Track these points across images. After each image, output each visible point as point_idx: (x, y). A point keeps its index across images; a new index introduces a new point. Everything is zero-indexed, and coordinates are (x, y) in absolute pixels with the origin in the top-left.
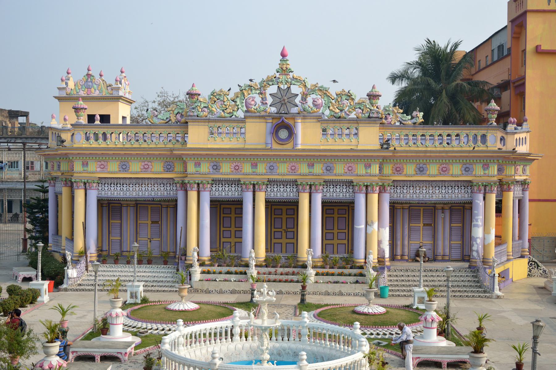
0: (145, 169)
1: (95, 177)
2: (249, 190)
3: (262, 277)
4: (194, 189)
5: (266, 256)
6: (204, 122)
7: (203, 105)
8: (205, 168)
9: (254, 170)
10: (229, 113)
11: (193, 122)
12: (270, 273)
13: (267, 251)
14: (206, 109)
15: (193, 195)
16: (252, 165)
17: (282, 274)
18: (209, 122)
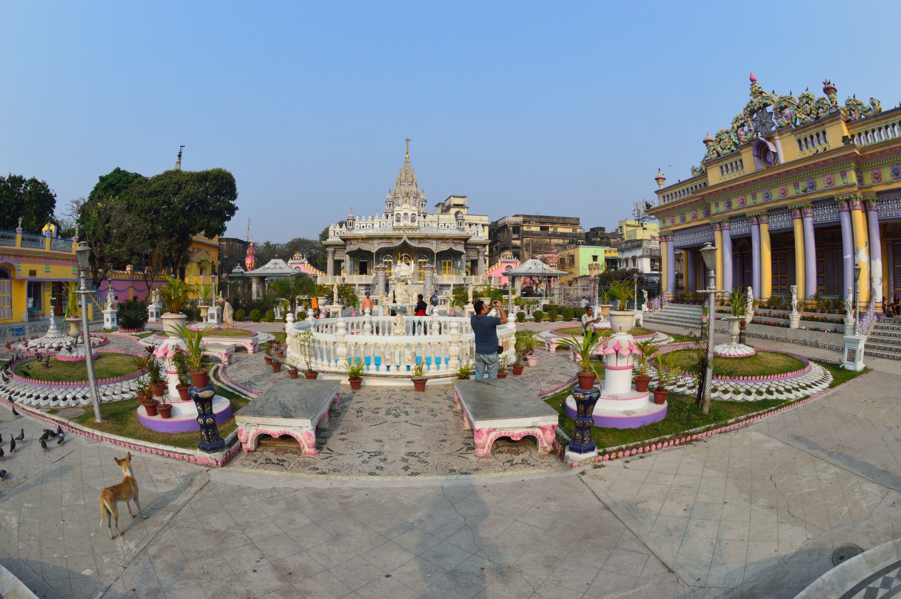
0: (695, 218)
1: (669, 231)
2: (754, 223)
3: (758, 318)
4: (717, 229)
5: (772, 298)
6: (715, 163)
7: (712, 149)
8: (722, 207)
9: (754, 201)
10: (729, 149)
11: (709, 165)
12: (765, 315)
13: (773, 290)
14: (715, 152)
15: (717, 234)
16: (752, 196)
17: (774, 316)
18: (718, 162)
